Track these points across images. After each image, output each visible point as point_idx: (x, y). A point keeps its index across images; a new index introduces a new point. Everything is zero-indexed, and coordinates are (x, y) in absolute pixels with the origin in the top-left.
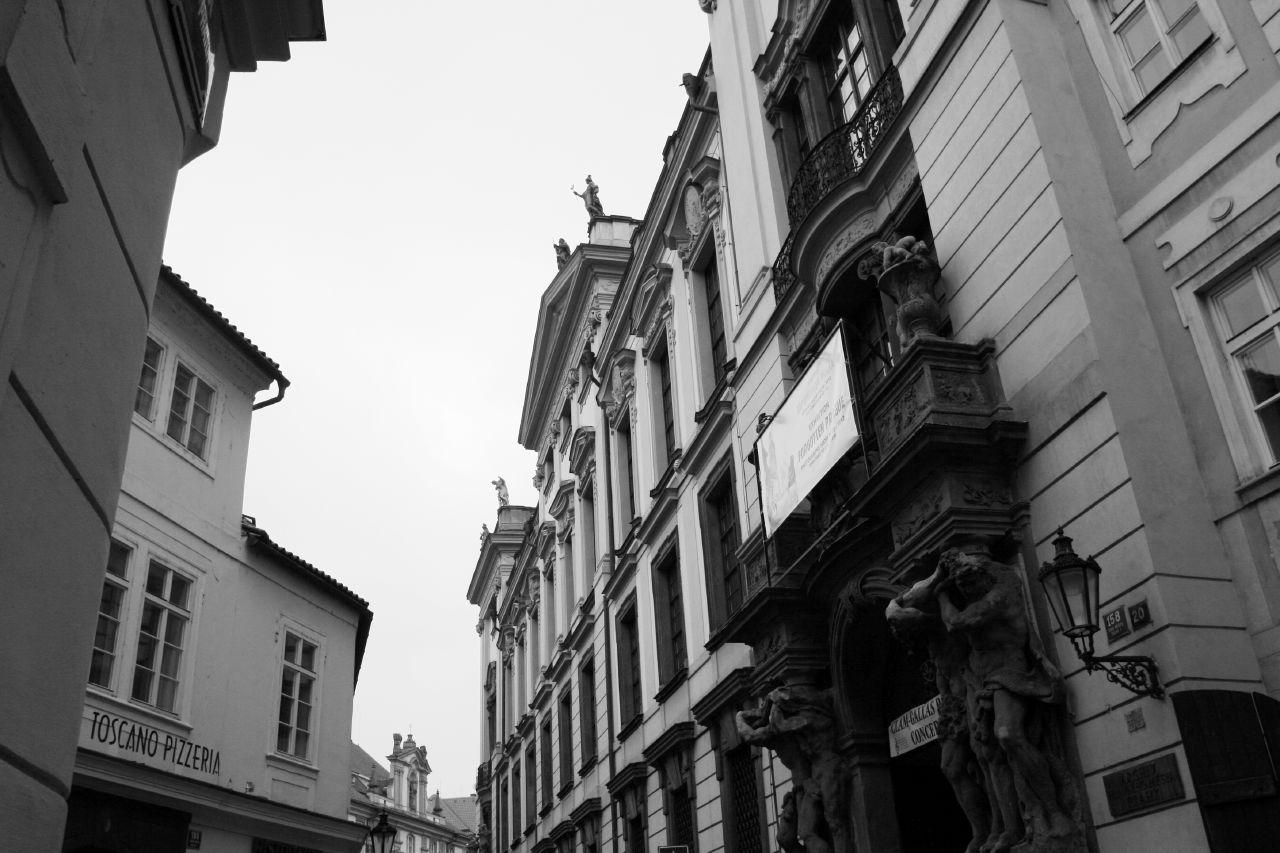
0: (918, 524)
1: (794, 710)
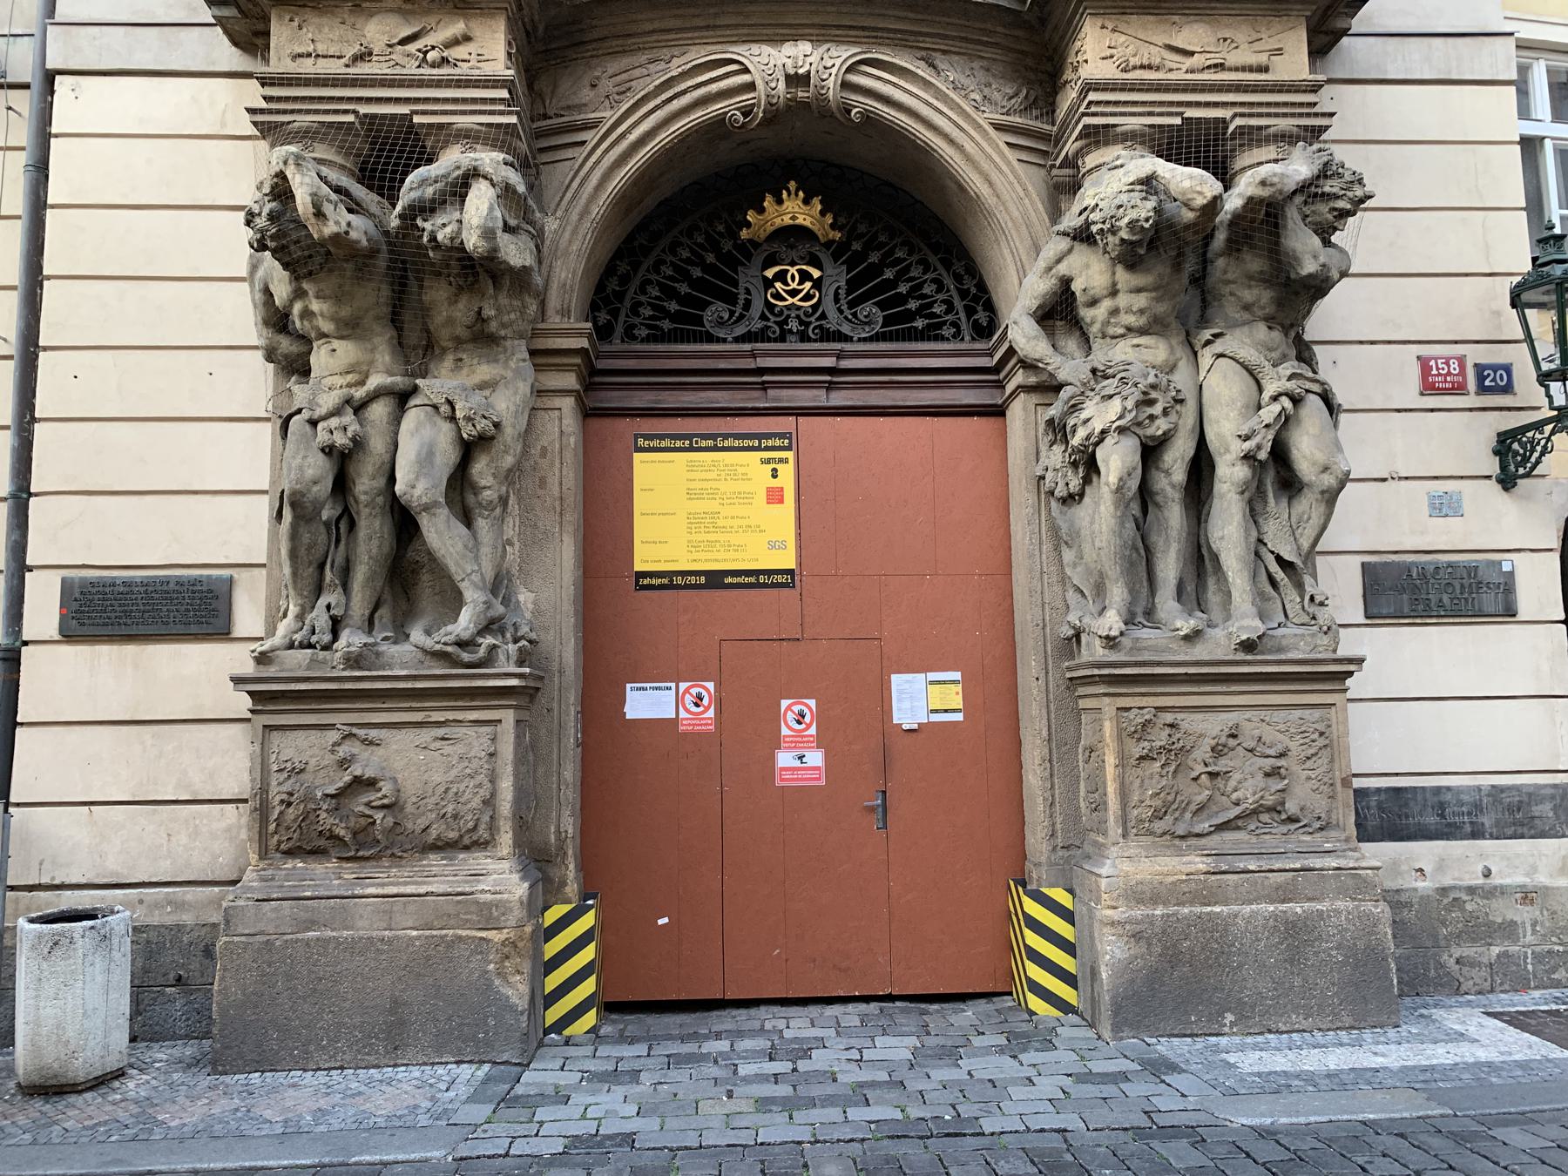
0: (1197, 61)
1: (513, 222)
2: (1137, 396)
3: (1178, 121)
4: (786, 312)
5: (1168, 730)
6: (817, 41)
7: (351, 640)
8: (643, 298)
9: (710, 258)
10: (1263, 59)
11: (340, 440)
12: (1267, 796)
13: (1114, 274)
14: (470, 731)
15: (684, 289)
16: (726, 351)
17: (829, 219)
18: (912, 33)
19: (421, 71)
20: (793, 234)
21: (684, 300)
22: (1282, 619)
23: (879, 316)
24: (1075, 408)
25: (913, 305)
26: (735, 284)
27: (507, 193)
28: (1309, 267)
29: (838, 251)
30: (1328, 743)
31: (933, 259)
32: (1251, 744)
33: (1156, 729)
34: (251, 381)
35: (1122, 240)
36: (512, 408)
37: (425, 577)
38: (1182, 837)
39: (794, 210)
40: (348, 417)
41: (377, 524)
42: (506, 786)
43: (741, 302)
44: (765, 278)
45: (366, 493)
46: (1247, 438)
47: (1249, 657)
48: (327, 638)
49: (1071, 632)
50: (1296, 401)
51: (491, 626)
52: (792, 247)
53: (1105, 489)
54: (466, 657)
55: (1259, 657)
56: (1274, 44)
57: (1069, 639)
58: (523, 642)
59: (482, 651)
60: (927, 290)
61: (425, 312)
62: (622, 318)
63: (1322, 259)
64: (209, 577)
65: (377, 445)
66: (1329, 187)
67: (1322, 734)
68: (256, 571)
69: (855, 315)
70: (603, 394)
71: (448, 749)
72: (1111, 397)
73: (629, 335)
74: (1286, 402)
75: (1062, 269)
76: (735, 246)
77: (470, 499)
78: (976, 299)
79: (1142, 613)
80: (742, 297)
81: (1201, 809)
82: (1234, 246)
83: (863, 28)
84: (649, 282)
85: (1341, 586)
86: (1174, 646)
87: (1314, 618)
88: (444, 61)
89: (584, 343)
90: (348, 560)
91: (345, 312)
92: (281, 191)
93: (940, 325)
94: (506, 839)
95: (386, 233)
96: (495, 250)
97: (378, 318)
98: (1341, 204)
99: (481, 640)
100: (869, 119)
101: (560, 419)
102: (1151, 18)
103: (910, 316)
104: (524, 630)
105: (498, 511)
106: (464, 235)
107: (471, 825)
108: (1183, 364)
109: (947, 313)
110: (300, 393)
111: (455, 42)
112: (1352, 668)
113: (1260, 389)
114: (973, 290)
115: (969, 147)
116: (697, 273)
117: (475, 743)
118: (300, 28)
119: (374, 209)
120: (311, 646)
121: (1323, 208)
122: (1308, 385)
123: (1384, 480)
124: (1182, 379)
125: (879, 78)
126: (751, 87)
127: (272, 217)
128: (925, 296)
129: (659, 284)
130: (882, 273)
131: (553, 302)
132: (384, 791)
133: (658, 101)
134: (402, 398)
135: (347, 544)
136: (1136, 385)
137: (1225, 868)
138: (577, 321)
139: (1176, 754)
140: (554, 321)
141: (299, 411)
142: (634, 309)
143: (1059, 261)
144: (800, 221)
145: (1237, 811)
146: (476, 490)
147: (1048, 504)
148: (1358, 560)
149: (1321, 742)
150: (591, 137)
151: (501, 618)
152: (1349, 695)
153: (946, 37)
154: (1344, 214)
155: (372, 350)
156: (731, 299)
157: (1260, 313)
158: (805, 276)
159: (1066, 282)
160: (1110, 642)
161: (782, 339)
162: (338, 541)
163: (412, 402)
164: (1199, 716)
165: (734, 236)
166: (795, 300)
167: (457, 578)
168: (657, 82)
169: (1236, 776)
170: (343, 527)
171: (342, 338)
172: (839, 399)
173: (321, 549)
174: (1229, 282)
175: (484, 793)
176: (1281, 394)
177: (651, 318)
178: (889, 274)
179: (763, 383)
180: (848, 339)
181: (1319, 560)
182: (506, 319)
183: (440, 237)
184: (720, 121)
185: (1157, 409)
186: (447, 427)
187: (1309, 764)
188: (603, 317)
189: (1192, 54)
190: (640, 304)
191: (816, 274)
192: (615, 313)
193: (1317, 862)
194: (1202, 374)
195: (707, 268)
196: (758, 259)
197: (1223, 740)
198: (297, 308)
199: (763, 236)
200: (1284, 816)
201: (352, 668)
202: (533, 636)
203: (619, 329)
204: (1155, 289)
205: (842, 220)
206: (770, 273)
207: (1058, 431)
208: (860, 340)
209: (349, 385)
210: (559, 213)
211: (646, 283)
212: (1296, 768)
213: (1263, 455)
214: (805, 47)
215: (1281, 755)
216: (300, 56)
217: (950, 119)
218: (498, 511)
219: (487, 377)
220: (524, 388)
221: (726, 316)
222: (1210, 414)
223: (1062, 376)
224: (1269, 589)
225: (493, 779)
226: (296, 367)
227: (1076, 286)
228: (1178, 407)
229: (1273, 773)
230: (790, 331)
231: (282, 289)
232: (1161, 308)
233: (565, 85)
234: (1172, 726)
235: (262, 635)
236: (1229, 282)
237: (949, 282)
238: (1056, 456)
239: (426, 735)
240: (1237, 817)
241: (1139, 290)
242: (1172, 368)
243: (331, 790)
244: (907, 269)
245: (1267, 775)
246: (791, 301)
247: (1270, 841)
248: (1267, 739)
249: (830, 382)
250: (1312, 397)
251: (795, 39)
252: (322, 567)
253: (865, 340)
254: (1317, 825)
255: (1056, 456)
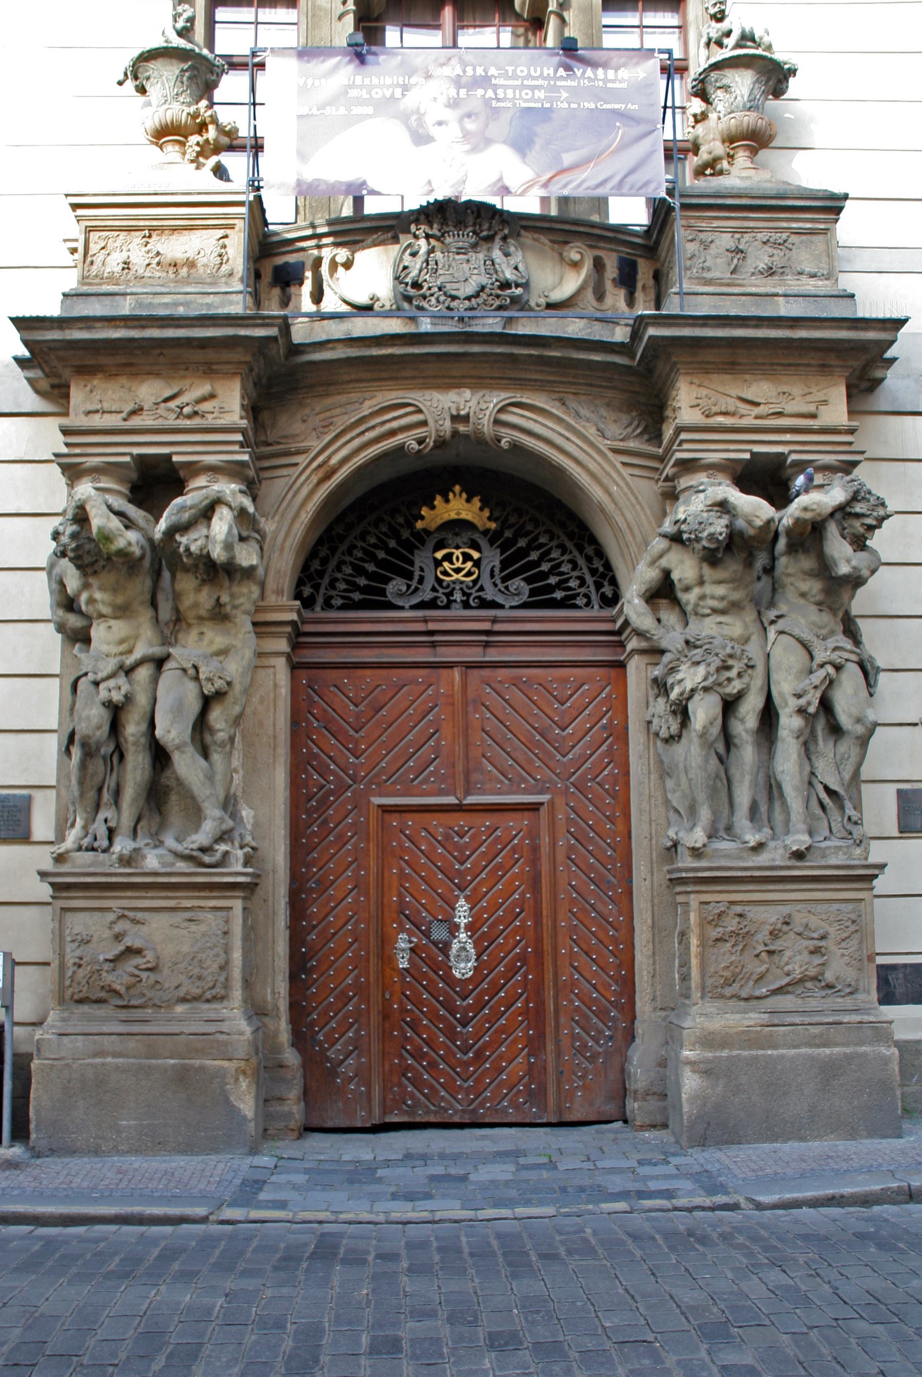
1: (245, 534)
2: (717, 662)
3: (747, 456)
4: (452, 586)
5: (737, 919)
6: (474, 387)
7: (123, 845)
8: (339, 576)
9: (392, 544)
10: (812, 408)
11: (117, 697)
12: (811, 969)
13: (701, 568)
14: (210, 916)
15: (371, 567)
16: (405, 618)
17: (486, 513)
18: (548, 382)
19: (179, 422)
20: (458, 526)
21: (370, 576)
22: (827, 833)
23: (526, 588)
24: (673, 670)
25: (553, 580)
26: (412, 563)
27: (242, 514)
28: (844, 569)
29: (493, 538)
30: (860, 928)
31: (569, 545)
32: (799, 929)
33: (728, 918)
34: (46, 647)
35: (704, 548)
36: (240, 670)
37: (174, 798)
38: (746, 999)
39: (457, 507)
40: (121, 680)
41: (140, 758)
42: (237, 956)
43: (416, 578)
44: (435, 559)
45: (133, 735)
46: (799, 696)
47: (798, 864)
48: (105, 843)
49: (670, 844)
50: (838, 668)
51: (223, 836)
52: (456, 534)
53: (693, 734)
54: (207, 859)
55: (807, 864)
56: (820, 396)
57: (668, 849)
58: (247, 849)
59: (218, 855)
60: (565, 568)
61: (177, 596)
62: (322, 591)
63: (854, 563)
64: (14, 795)
65: (142, 700)
66: (859, 508)
67: (854, 922)
68: (48, 791)
69: (507, 588)
70: (305, 652)
71: (193, 927)
72: (698, 663)
73: (328, 605)
74: (830, 669)
75: (664, 562)
76: (412, 534)
77: (208, 738)
78: (603, 576)
79: (721, 828)
80: (417, 574)
81: (761, 977)
82: (794, 548)
83: (510, 379)
84: (344, 562)
85: (880, 808)
86: (745, 854)
87: (851, 833)
88: (196, 413)
89: (294, 616)
90: (118, 785)
91: (120, 600)
92: (81, 517)
93: (574, 597)
94: (237, 994)
95: (150, 540)
96: (233, 558)
97: (143, 603)
98: (869, 521)
99: (217, 847)
100: (516, 447)
101: (275, 674)
102: (728, 376)
103: (551, 589)
104: (248, 839)
105: (228, 747)
106: (210, 547)
107: (210, 984)
108: (754, 638)
109: (580, 586)
110: (86, 661)
111: (204, 399)
112: (876, 872)
113: (812, 658)
114: (601, 569)
115: (592, 466)
116: (381, 555)
117: (213, 924)
118: (91, 391)
119: (141, 522)
120: (93, 849)
121: (857, 524)
122: (846, 655)
123: (916, 724)
124: (753, 650)
125: (522, 416)
126: (424, 423)
127: (74, 536)
128: (562, 574)
129: (352, 564)
130: (528, 555)
131: (271, 585)
132: (148, 958)
133: (354, 433)
134: (159, 663)
135: (118, 772)
136: (717, 655)
137: (776, 1022)
138: (288, 600)
139: (742, 937)
140: (272, 599)
141: (86, 674)
142: (332, 585)
143: (661, 556)
144: (465, 515)
145: (787, 980)
146: (212, 732)
147: (655, 743)
148: (894, 787)
149: (853, 928)
150: (302, 460)
151: (231, 830)
152: (875, 892)
153: (575, 384)
154: (871, 528)
155: (138, 627)
156: (409, 575)
157: (812, 600)
158: (467, 557)
159: (667, 573)
160: (696, 853)
161: (447, 607)
162: (112, 770)
163: (169, 665)
164: (762, 908)
165: (411, 526)
166: (459, 576)
167: (200, 800)
168: (353, 420)
169: (788, 953)
170: (115, 759)
171: (116, 618)
172: (493, 655)
173: (101, 776)
174: (789, 575)
175: (221, 959)
176: (825, 663)
177: (345, 591)
178: (534, 556)
179: (433, 642)
180: (501, 607)
181: (864, 787)
182: (237, 602)
183: (193, 548)
184: (401, 448)
185: (733, 673)
186: (192, 686)
187: (843, 944)
188: (307, 591)
189: (757, 404)
190: (337, 580)
191: (476, 555)
192: (316, 587)
193: (846, 1019)
194: (770, 645)
195: (389, 551)
196: (431, 544)
197: (779, 926)
198: (84, 597)
199: (433, 526)
200: (823, 984)
201: (124, 866)
202: (254, 844)
203: (320, 600)
204: (732, 581)
205: (496, 514)
206: (439, 555)
207: (661, 686)
208: (512, 608)
209: (121, 654)
210: (277, 518)
211: (341, 563)
212: (833, 948)
213: (812, 710)
214: (467, 393)
215: (823, 938)
216: (90, 412)
217: (577, 446)
218: (228, 747)
219: (222, 647)
220: (248, 653)
221: (404, 588)
222: (774, 677)
223: (664, 644)
224: (818, 811)
225: (227, 950)
226: (79, 637)
227: (675, 576)
228: (750, 671)
229: (815, 951)
230: (455, 601)
231: (73, 582)
232: (736, 596)
233: (283, 420)
234: (740, 915)
235: (53, 839)
236: (789, 575)
237: (581, 562)
238: (660, 706)
239: (179, 917)
240: (788, 985)
241: (720, 582)
242: (747, 640)
243: (110, 956)
244: (548, 552)
245: (812, 953)
246: (455, 576)
247: (813, 1004)
248: (812, 926)
249: (487, 642)
250: (849, 664)
251: (458, 386)
252: (100, 790)
253: (512, 608)
254: (848, 990)
255: (660, 706)
